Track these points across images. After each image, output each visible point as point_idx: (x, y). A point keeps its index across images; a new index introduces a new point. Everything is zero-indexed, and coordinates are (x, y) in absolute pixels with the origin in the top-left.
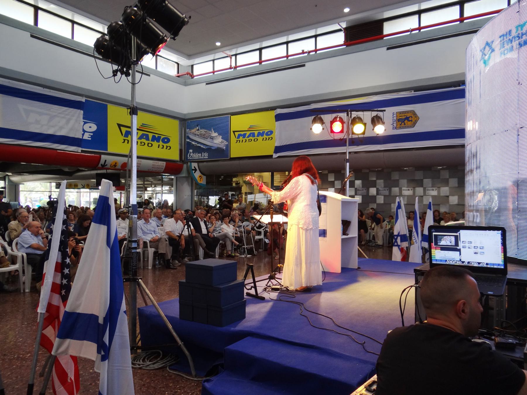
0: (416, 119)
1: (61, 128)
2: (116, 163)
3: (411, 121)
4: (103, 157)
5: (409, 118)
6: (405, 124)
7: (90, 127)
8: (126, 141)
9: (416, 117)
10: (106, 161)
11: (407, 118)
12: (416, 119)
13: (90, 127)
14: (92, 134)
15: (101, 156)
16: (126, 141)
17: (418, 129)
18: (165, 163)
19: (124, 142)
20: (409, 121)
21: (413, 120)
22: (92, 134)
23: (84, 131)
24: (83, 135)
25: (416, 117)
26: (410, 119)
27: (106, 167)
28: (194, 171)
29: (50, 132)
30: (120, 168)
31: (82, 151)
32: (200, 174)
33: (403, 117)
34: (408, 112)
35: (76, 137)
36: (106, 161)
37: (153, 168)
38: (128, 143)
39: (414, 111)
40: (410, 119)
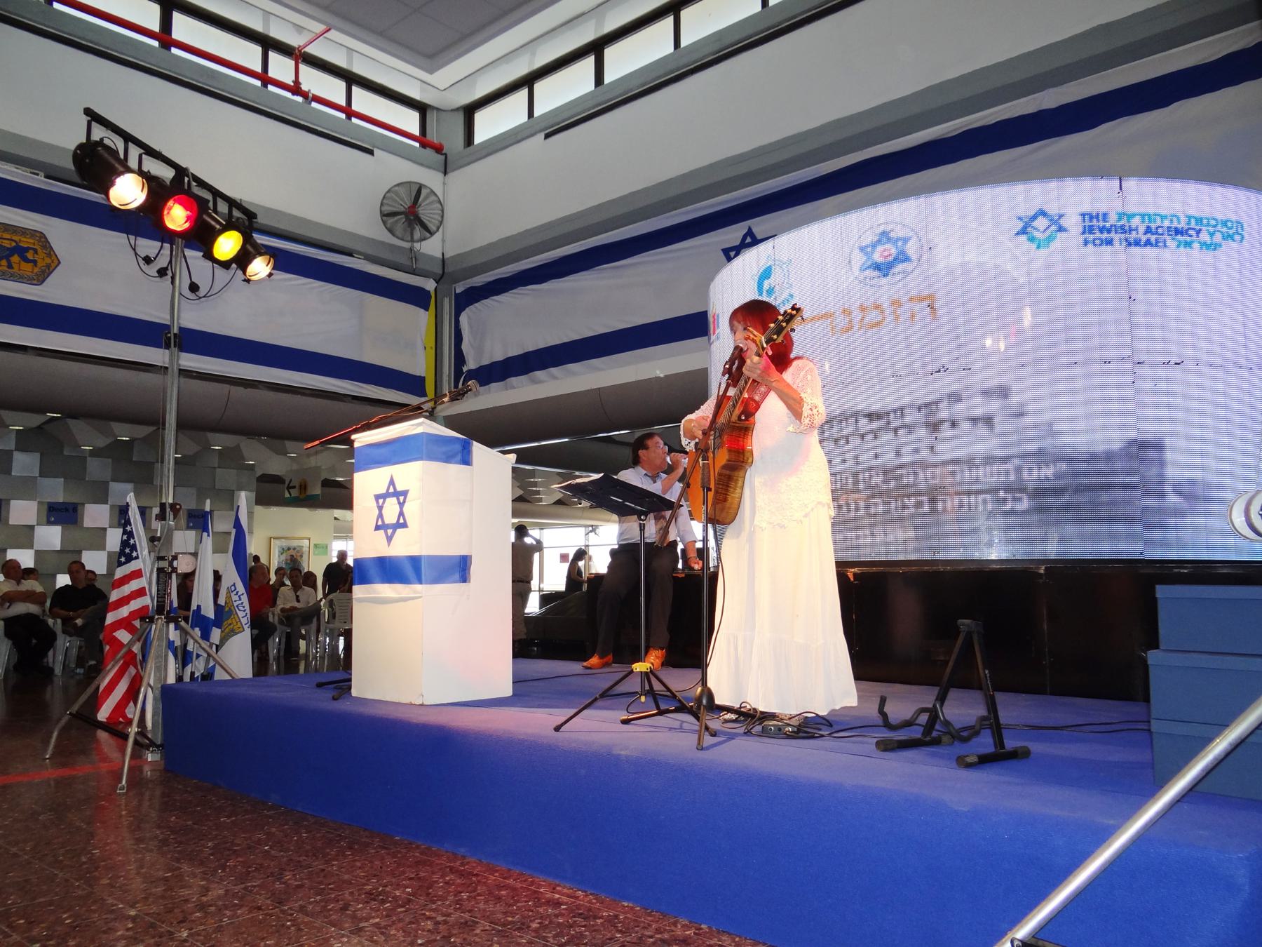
0: (48, 261)
3: (35, 262)
5: (27, 249)
6: (10, 266)
9: (49, 255)
11: (21, 251)
12: (48, 261)
17: (52, 292)
20: (27, 260)
21: (40, 264)
25: (49, 255)
26: (30, 255)
33: (7, 244)
34: (24, 232)
39: (42, 236)
40: (30, 255)
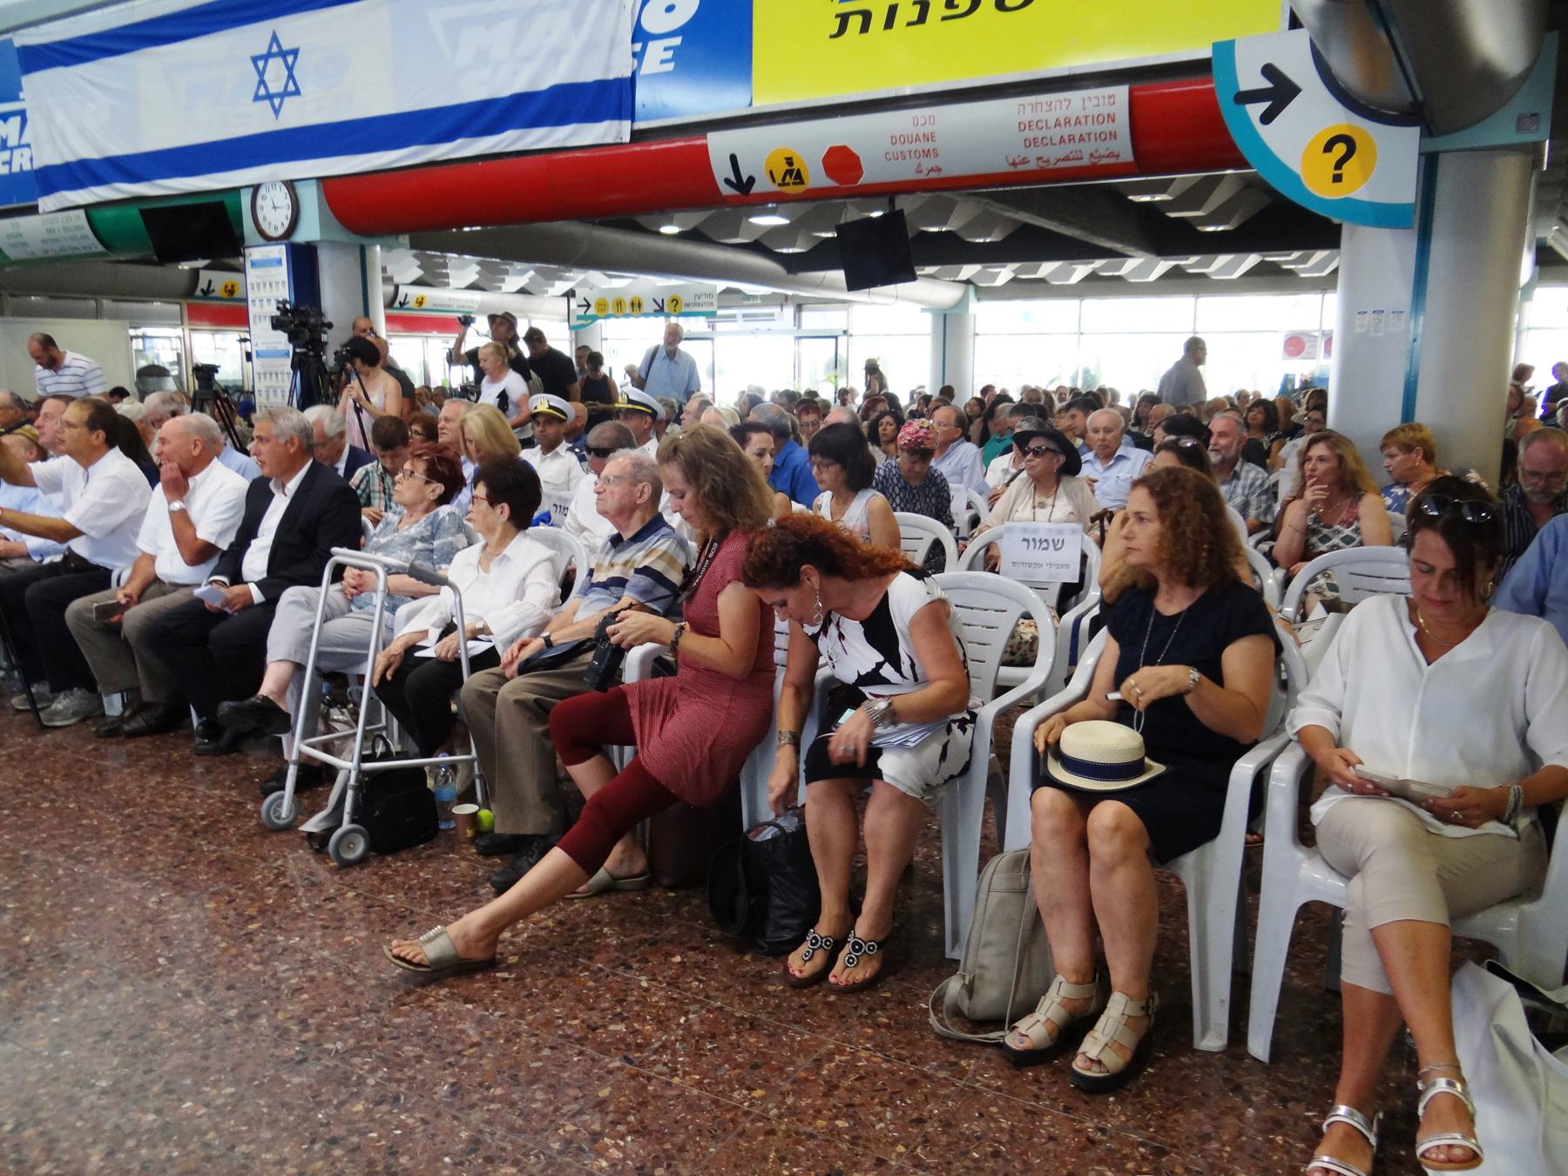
1: (556, 54)
2: (789, 161)
4: (719, 145)
7: (670, 9)
8: (855, 22)
10: (733, 158)
13: (670, 9)
14: (677, 41)
15: (705, 147)
16: (855, 22)
18: (1121, 92)
19: (842, 29)
22: (677, 41)
23: (640, 35)
24: (638, 56)
27: (756, 189)
28: (1255, 110)
29: (519, 86)
30: (827, 182)
31: (637, 136)
32: (1339, 118)
35: (611, 76)
36: (733, 158)
37: (1029, 143)
38: (865, 28)
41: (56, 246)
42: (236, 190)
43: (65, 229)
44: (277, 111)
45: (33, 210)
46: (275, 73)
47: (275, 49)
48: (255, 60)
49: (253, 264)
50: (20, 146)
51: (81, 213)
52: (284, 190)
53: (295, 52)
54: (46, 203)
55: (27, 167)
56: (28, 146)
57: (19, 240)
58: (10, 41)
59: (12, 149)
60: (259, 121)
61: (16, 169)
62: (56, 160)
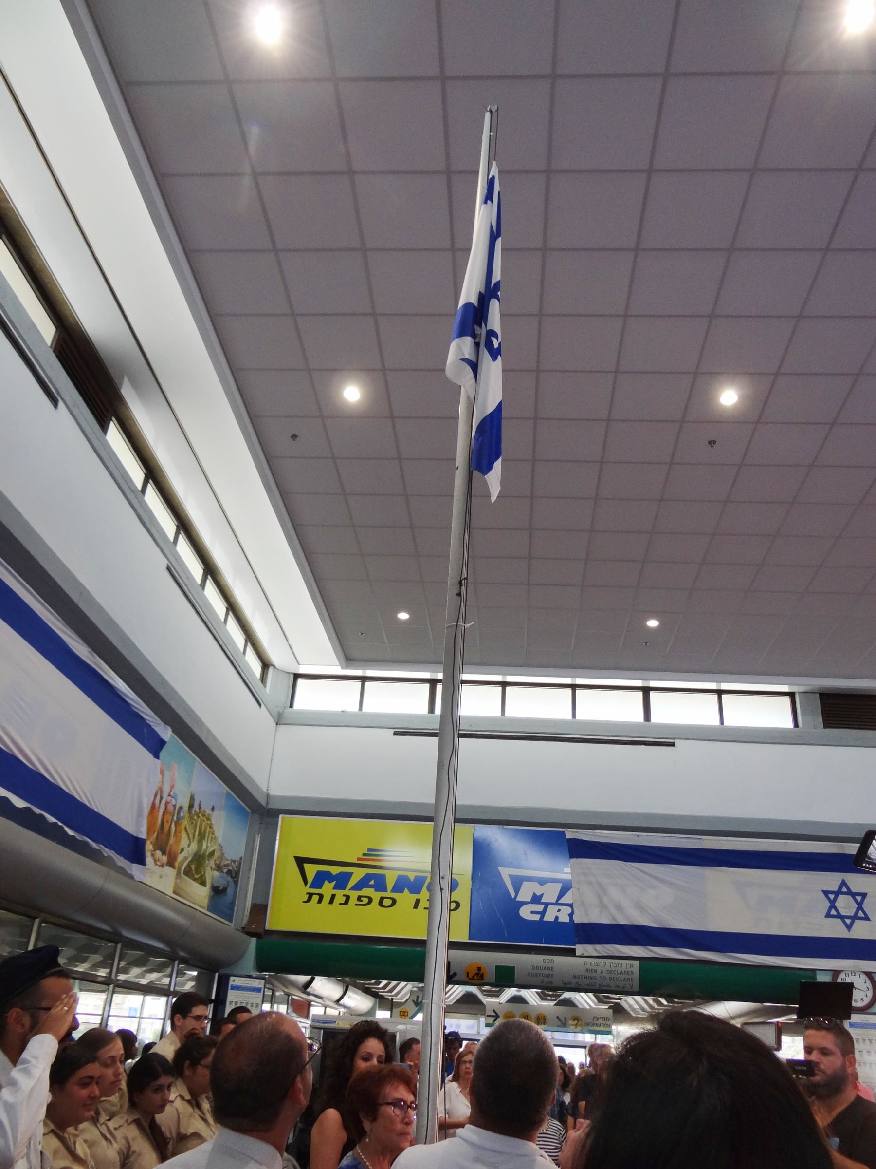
41: (574, 981)
42: (814, 971)
43: (609, 972)
44: (849, 927)
45: (572, 953)
46: (845, 905)
47: (844, 889)
48: (826, 893)
49: (851, 1025)
50: (557, 904)
51: (636, 963)
52: (864, 977)
53: (864, 895)
54: (580, 949)
55: (564, 918)
56: (571, 906)
57: (547, 972)
58: (563, 833)
59: (547, 905)
60: (834, 930)
61: (549, 917)
62: (605, 920)
